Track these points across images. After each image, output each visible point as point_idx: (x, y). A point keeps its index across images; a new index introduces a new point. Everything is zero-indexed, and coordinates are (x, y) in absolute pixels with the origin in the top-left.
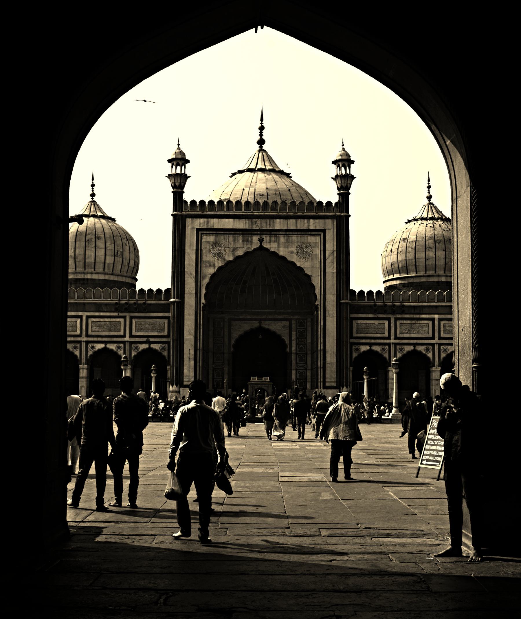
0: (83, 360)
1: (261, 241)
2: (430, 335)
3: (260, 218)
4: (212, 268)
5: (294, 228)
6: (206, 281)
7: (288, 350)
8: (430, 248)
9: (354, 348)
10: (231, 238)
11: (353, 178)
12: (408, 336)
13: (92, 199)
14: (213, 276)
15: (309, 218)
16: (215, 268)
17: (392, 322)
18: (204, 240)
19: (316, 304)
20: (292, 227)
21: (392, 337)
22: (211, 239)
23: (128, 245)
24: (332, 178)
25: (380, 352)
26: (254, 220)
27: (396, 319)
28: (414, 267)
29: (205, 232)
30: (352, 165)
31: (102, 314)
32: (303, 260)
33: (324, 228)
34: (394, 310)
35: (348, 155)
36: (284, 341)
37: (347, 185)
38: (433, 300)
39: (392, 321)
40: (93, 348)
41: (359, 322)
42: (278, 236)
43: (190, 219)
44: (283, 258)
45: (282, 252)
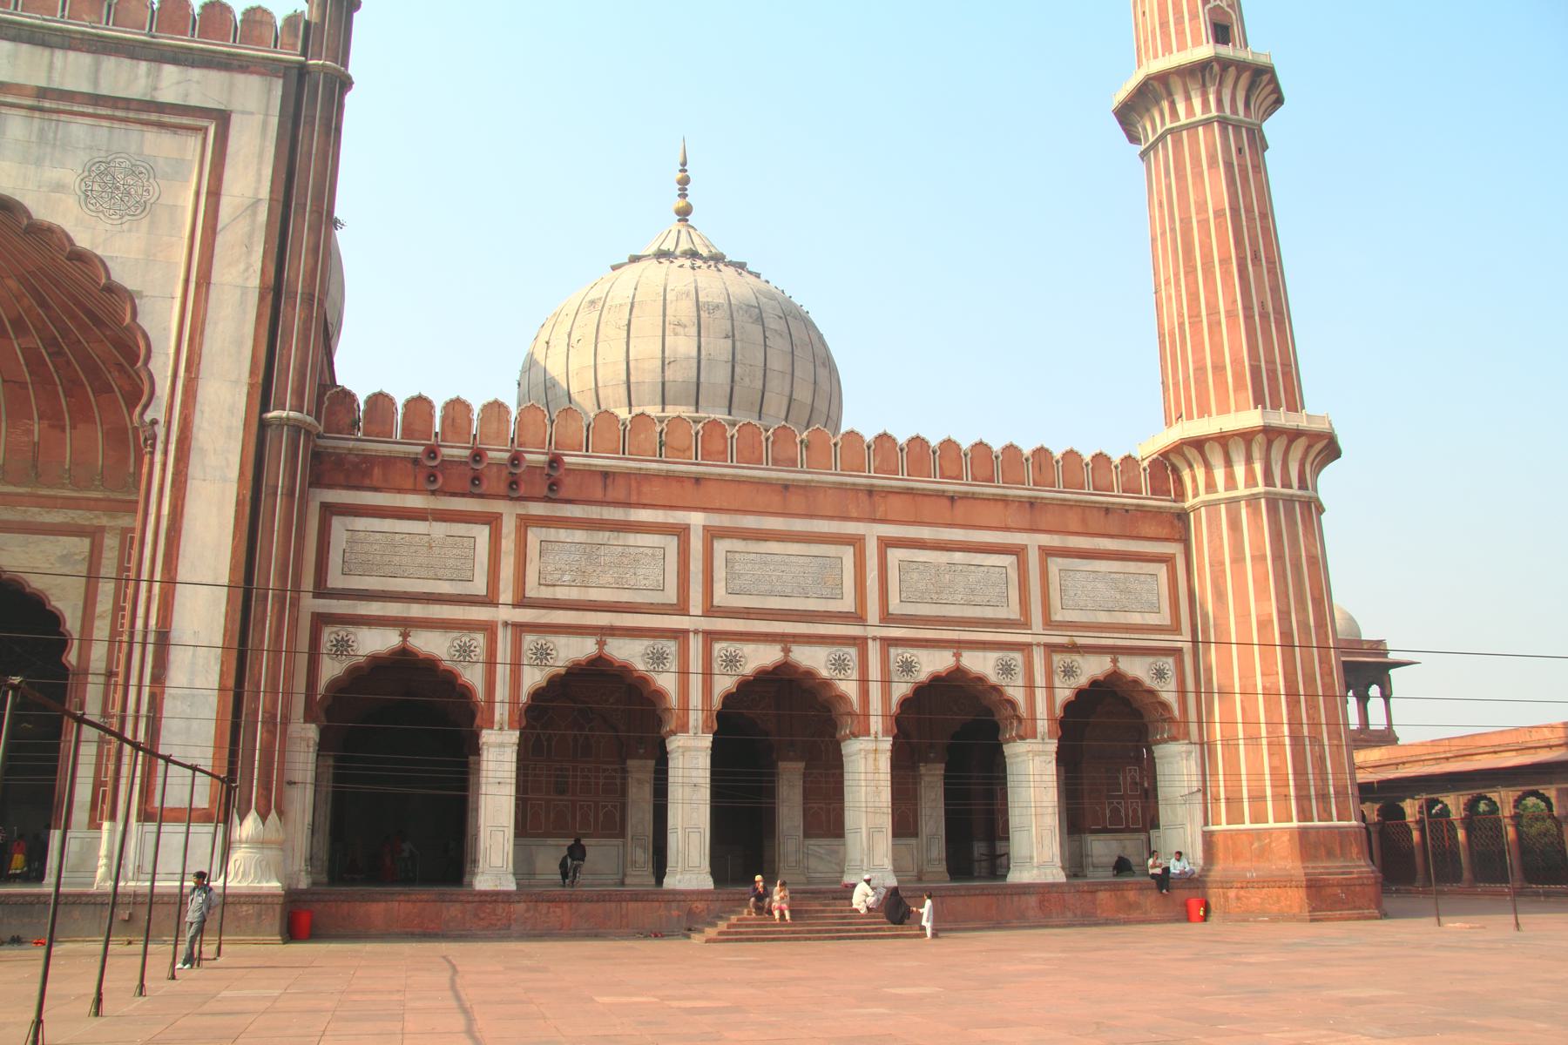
2: (671, 596)
7: (72, 657)
8: (679, 325)
9: (329, 635)
12: (574, 594)
17: (505, 531)
19: (148, 417)
21: (506, 595)
27: (525, 522)
28: (625, 386)
32: (108, 227)
33: (223, 108)
36: (53, 620)
38: (684, 451)
39: (509, 527)
41: (362, 523)
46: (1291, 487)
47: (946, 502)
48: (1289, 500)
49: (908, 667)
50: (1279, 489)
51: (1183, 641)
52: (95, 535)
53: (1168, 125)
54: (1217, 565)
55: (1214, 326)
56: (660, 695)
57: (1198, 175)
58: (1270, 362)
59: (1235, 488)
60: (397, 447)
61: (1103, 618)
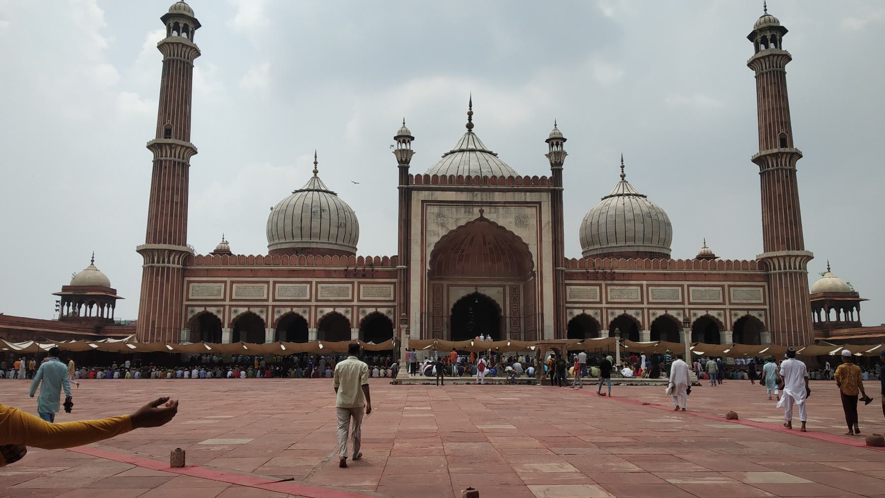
0: (313, 324)
1: (482, 212)
3: (481, 191)
4: (437, 237)
5: (512, 201)
6: (430, 249)
7: (502, 314)
10: (454, 209)
11: (566, 154)
13: (315, 175)
14: (437, 244)
15: (526, 191)
16: (439, 236)
18: (428, 211)
19: (534, 270)
20: (510, 201)
21: (604, 302)
22: (434, 210)
23: (349, 216)
24: (545, 155)
25: (593, 316)
26: (476, 193)
27: (607, 285)
29: (430, 204)
30: (564, 143)
31: (331, 280)
34: (604, 276)
35: (560, 134)
36: (498, 305)
37: (560, 161)
40: (322, 312)
41: (573, 287)
42: (497, 207)
43: (416, 192)
44: (502, 228)
45: (501, 222)
46: (796, 269)
47: (704, 275)
48: (796, 273)
49: (695, 315)
50: (793, 270)
51: (767, 307)
52: (504, 287)
53: (767, 169)
54: (776, 289)
55: (777, 226)
56: (639, 322)
57: (774, 184)
58: (792, 236)
59: (781, 269)
60: (580, 271)
61: (745, 302)
